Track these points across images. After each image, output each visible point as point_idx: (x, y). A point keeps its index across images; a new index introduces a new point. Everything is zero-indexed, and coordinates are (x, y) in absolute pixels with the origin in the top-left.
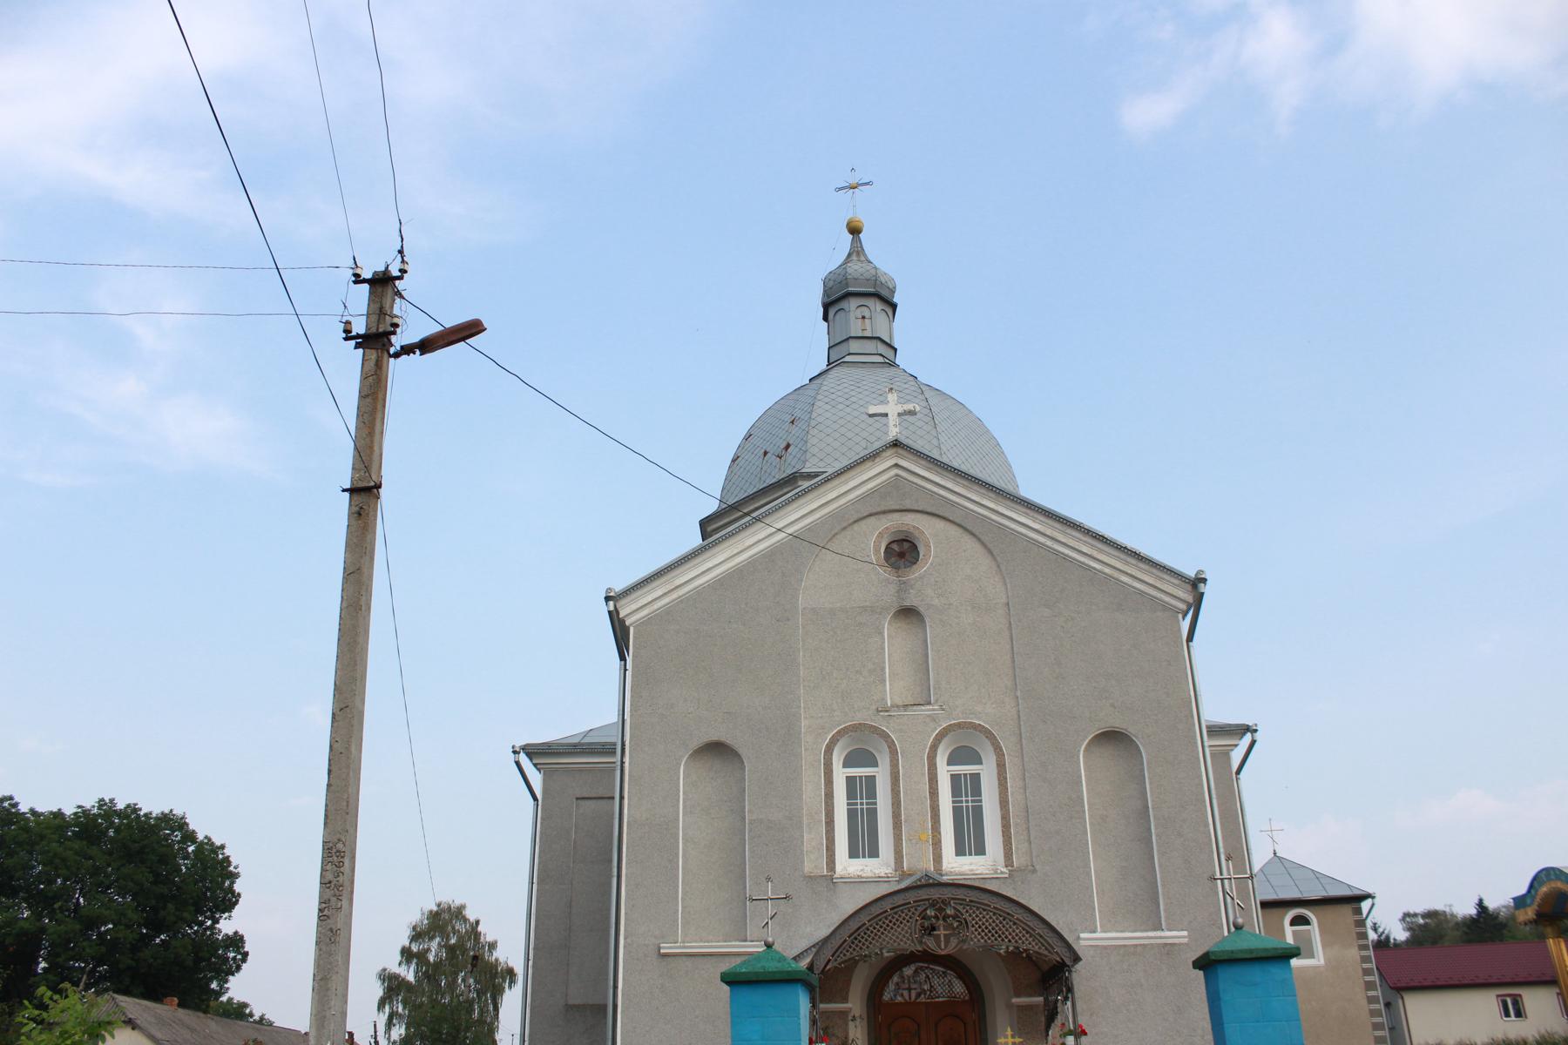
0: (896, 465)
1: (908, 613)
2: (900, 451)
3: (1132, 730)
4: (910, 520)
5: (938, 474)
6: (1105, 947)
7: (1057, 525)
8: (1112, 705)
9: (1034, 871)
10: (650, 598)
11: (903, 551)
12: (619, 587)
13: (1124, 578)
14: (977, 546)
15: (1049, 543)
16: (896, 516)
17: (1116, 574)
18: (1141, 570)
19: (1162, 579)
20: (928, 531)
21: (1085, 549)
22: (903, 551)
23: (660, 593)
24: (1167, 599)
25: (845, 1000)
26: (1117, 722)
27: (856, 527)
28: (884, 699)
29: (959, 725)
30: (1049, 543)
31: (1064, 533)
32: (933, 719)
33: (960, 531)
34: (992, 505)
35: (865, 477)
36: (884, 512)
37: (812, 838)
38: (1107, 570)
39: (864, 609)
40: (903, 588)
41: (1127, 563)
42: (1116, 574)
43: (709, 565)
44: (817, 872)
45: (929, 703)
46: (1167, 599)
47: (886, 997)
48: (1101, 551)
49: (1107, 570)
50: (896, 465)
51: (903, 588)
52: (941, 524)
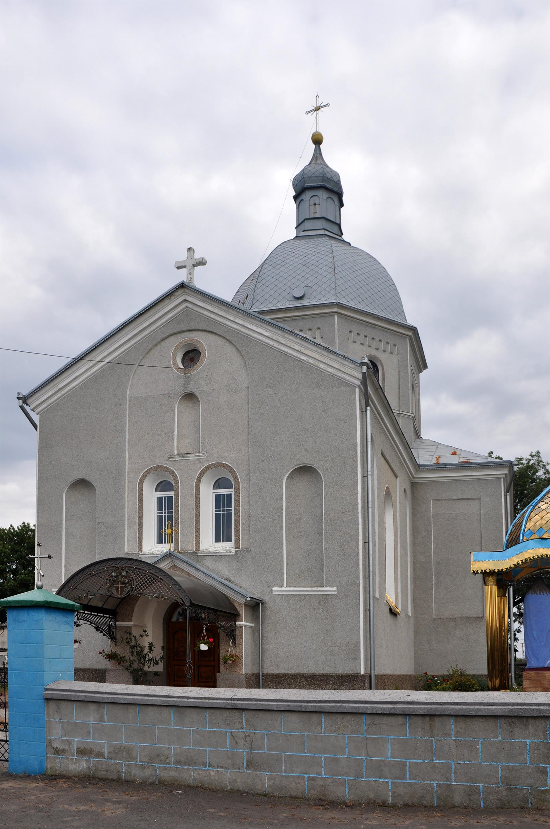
0: (185, 300)
1: (190, 397)
2: (186, 290)
3: (316, 466)
4: (194, 336)
5: (209, 304)
6: (287, 596)
7: (280, 332)
8: (306, 450)
9: (250, 551)
10: (45, 397)
11: (192, 356)
12: (25, 392)
13: (322, 366)
14: (234, 351)
15: (276, 345)
16: (186, 334)
17: (317, 363)
18: (331, 359)
19: (344, 364)
20: (205, 342)
21: (297, 347)
22: (192, 356)
23: (50, 393)
24: (348, 378)
25: (130, 620)
26: (307, 461)
27: (163, 344)
28: (172, 451)
29: (215, 465)
30: (276, 345)
31: (284, 337)
32: (200, 461)
33: (224, 341)
34: (241, 322)
35: (166, 310)
36: (180, 332)
37: (128, 533)
38: (311, 361)
39: (164, 395)
40: (187, 381)
41: (323, 355)
42: (317, 363)
43: (77, 374)
44: (133, 551)
45: (199, 452)
46: (348, 378)
47: (174, 619)
48: (307, 348)
49: (311, 361)
50: (185, 300)
51: (187, 381)
52: (212, 337)
